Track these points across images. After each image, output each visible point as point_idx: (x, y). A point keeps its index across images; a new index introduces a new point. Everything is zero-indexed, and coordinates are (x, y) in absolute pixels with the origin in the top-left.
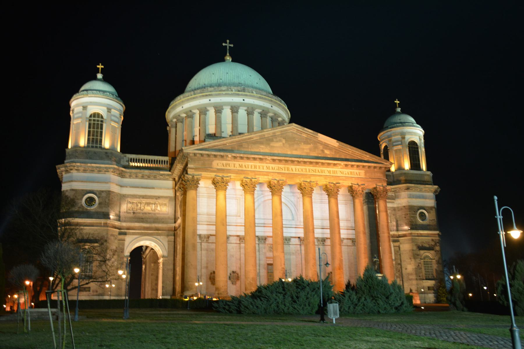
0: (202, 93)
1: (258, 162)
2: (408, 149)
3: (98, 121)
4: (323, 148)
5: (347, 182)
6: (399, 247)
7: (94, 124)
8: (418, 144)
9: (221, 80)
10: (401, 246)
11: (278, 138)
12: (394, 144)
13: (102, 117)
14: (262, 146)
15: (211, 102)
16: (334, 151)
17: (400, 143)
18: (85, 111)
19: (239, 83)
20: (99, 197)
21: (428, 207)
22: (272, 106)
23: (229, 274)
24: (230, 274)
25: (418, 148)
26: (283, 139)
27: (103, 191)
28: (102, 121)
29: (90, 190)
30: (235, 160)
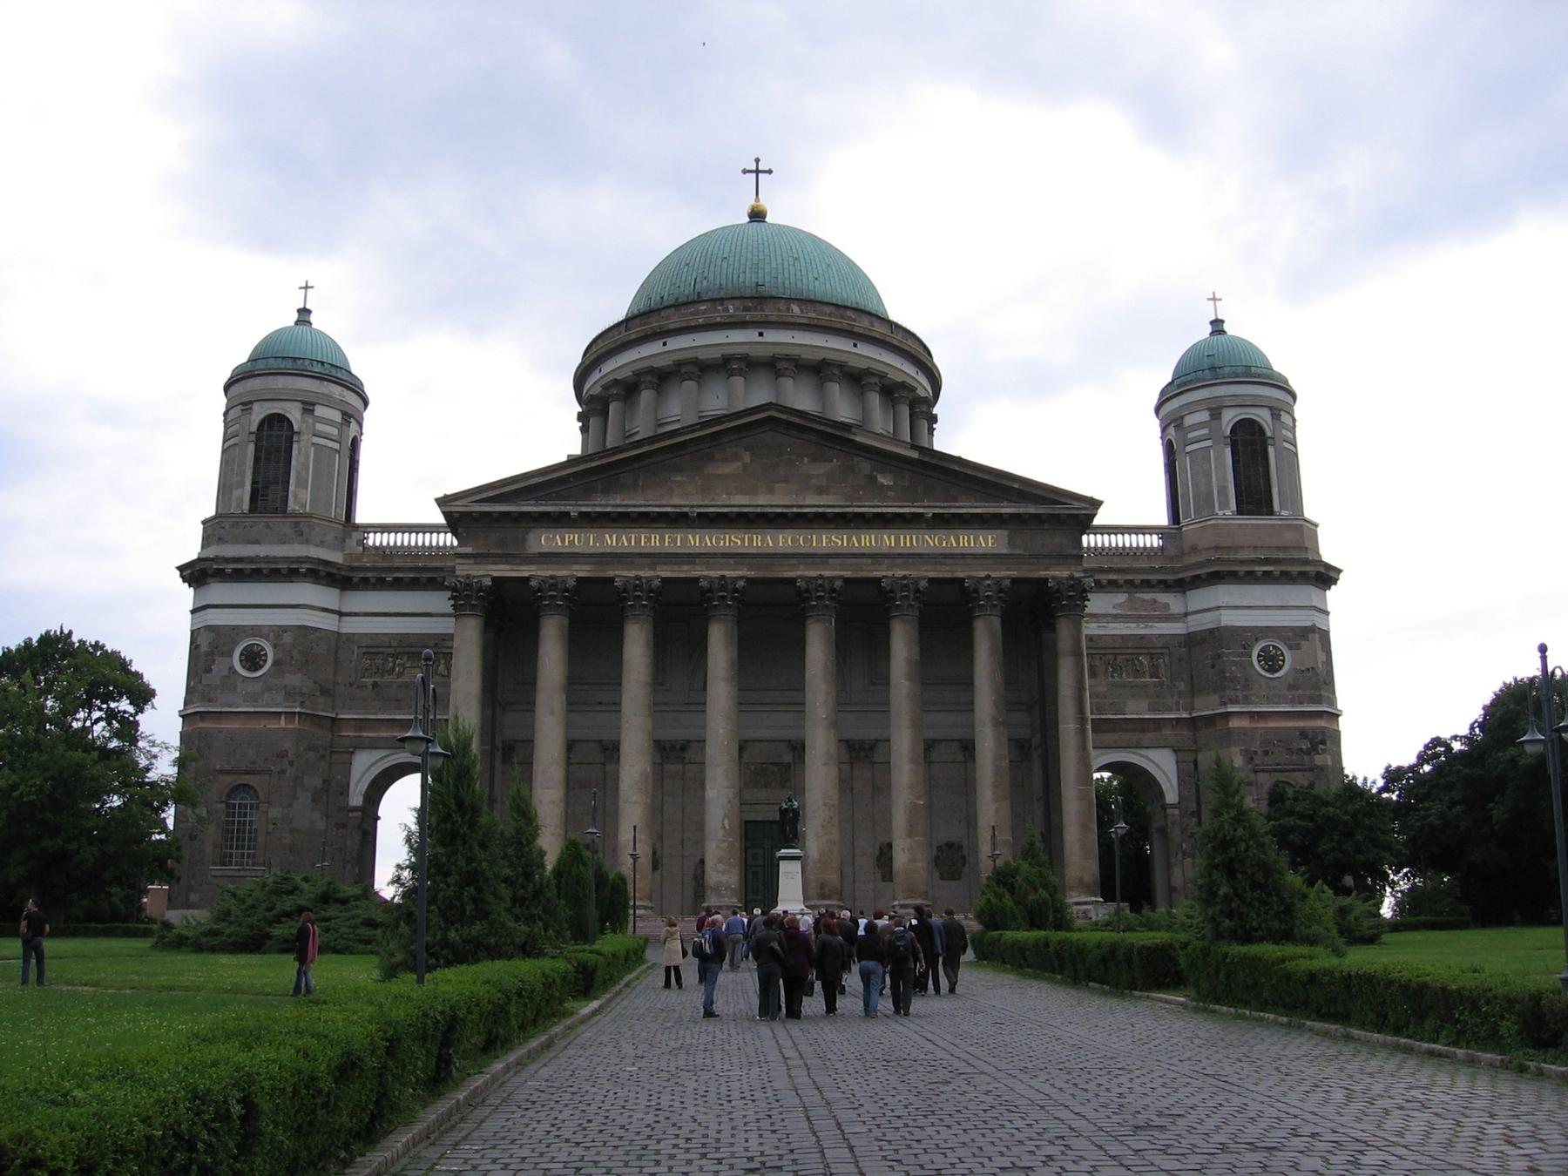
0: (645, 325)
2: (1228, 451)
4: (872, 472)
5: (947, 568)
6: (1195, 763)
8: (1269, 434)
9: (705, 281)
10: (1200, 757)
11: (728, 449)
12: (1191, 435)
14: (679, 478)
15: (666, 349)
17: (1206, 431)
19: (757, 285)
20: (275, 647)
21: (1292, 629)
22: (855, 345)
26: (746, 450)
27: (284, 629)
29: (252, 627)
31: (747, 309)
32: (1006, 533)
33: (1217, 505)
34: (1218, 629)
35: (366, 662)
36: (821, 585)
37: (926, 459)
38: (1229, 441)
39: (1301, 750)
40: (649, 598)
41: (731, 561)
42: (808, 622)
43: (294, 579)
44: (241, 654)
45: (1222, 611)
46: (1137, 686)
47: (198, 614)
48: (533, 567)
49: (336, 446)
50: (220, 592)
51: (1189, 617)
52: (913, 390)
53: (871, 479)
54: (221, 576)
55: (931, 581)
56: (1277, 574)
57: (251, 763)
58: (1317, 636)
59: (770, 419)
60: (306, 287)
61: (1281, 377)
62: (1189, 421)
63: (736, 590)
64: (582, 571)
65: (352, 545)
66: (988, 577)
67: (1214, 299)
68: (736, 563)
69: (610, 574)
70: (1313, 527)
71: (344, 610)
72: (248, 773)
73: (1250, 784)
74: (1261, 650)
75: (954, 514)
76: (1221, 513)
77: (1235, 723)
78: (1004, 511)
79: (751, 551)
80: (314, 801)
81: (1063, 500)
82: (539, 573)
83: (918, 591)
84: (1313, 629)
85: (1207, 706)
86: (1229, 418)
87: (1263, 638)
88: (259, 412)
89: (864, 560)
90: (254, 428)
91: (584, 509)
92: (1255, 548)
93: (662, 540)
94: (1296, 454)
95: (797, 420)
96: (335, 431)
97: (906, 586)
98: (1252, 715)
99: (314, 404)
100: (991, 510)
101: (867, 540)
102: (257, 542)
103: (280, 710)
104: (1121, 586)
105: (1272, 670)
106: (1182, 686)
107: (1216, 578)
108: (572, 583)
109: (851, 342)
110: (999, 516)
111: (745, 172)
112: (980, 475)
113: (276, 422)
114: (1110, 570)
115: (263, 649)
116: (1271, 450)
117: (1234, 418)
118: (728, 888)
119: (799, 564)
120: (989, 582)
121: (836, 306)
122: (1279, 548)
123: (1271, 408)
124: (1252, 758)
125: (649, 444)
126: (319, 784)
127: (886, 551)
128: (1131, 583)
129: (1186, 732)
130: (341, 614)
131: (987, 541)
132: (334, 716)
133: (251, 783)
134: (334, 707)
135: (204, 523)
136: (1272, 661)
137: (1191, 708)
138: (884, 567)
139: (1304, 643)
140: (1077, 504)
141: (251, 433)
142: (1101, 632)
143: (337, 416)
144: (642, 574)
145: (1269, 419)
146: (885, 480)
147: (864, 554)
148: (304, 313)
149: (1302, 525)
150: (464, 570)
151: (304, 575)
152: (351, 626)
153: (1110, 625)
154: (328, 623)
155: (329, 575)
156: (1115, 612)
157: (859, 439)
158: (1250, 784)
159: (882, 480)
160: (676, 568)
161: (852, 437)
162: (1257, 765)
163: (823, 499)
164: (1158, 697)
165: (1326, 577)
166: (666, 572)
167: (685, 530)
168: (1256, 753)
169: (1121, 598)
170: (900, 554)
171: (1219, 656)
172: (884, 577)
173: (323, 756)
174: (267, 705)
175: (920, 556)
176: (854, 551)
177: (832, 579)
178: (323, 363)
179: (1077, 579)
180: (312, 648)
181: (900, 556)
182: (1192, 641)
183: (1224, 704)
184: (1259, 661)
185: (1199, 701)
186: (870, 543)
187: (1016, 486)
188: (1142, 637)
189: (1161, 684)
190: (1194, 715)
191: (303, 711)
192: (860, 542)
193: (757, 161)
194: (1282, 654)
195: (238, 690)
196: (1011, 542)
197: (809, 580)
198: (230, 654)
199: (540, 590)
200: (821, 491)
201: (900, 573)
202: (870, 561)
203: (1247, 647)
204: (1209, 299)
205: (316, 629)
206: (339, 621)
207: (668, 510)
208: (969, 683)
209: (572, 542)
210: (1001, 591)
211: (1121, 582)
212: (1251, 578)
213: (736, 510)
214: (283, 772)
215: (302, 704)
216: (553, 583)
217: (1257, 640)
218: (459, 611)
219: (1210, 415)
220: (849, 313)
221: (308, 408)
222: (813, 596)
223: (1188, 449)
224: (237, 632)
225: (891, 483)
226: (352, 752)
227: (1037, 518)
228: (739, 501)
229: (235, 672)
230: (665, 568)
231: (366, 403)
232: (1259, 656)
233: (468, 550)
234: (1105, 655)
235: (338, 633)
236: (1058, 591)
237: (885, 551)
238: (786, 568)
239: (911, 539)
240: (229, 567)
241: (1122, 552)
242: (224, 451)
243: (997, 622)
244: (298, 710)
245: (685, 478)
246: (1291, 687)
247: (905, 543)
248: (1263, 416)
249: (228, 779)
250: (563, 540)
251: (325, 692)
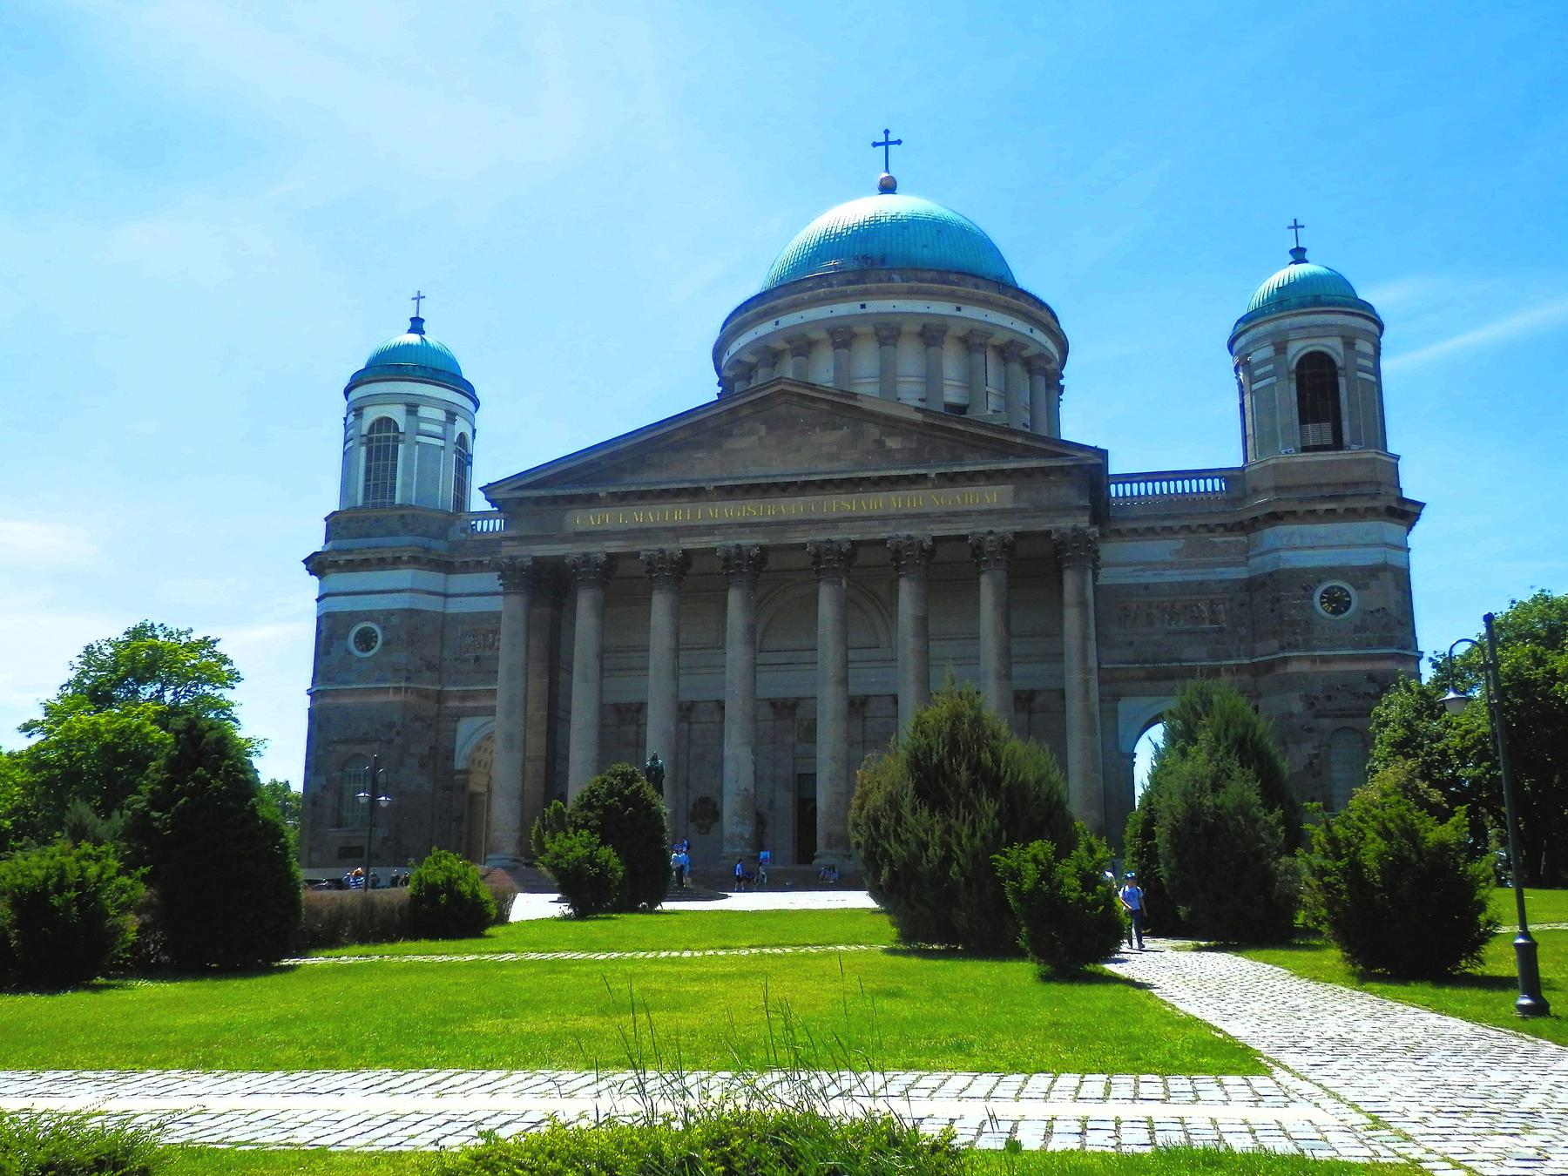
1: (685, 500)
2: (1293, 386)
3: (387, 438)
5: (953, 526)
7: (378, 447)
8: (1339, 363)
12: (1258, 372)
13: (396, 428)
14: (700, 455)
16: (915, 438)
17: (1270, 367)
18: (358, 421)
20: (384, 629)
21: (1361, 569)
22: (959, 309)
23: (691, 808)
24: (694, 806)
25: (1335, 376)
27: (390, 613)
28: (396, 440)
29: (364, 612)
30: (623, 503)
31: (849, 283)
32: (1010, 487)
33: (1280, 444)
34: (1277, 572)
35: (469, 640)
37: (930, 421)
38: (1294, 376)
39: (1369, 694)
40: (672, 569)
41: (747, 530)
42: (821, 584)
43: (401, 566)
44: (356, 637)
45: (1284, 554)
46: (1195, 633)
47: (323, 601)
48: (570, 546)
49: (440, 443)
50: (340, 581)
51: (1250, 561)
52: (1024, 347)
53: (880, 443)
54: (337, 567)
55: (934, 539)
56: (1341, 511)
57: (364, 734)
58: (1389, 575)
59: (783, 392)
60: (418, 298)
61: (1367, 306)
62: (1254, 358)
63: (750, 558)
64: (613, 547)
65: (456, 535)
66: (991, 533)
67: (1296, 226)
68: (751, 532)
69: (637, 548)
70: (1394, 461)
71: (451, 591)
72: (361, 741)
73: (1310, 730)
74: (1325, 592)
75: (956, 473)
76: (1283, 451)
77: (1293, 668)
78: (1005, 466)
79: (766, 519)
80: (421, 766)
81: (1066, 452)
82: (575, 550)
83: (922, 550)
84: (1385, 567)
85: (1267, 650)
86: (1297, 349)
87: (1326, 579)
88: (372, 414)
89: (873, 522)
90: (365, 431)
91: (611, 490)
92: (1320, 485)
93: (684, 514)
94: (1379, 384)
95: (807, 392)
96: (438, 430)
97: (909, 545)
98: (1313, 660)
99: (417, 406)
100: (994, 467)
101: (876, 502)
102: (368, 535)
103: (388, 685)
104: (1177, 533)
105: (1336, 612)
106: (1243, 631)
107: (1275, 518)
108: (603, 557)
109: (955, 305)
110: (1003, 471)
111: (875, 144)
112: (983, 432)
113: (385, 423)
114: (1165, 518)
115: (374, 631)
116: (1342, 381)
117: (1299, 351)
118: (743, 838)
120: (992, 538)
121: (938, 271)
122: (1346, 485)
123: (1343, 337)
124: (1313, 704)
125: (669, 425)
126: (426, 751)
128: (1188, 528)
129: (1246, 677)
130: (446, 595)
131: (993, 496)
132: (439, 688)
133: (364, 752)
134: (440, 682)
135: (326, 519)
136: (1338, 602)
137: (1252, 655)
138: (891, 528)
139: (1373, 583)
140: (1080, 455)
141: (362, 436)
142: (1157, 580)
143: (440, 415)
144: (665, 546)
145: (1340, 349)
146: (893, 443)
148: (417, 325)
149: (1375, 459)
150: (508, 550)
151: (408, 562)
152: (455, 607)
153: (1168, 572)
154: (432, 605)
155: (430, 561)
156: (1172, 559)
157: (866, 405)
158: (1310, 730)
159: (890, 444)
160: (697, 539)
161: (858, 404)
162: (1318, 711)
163: (836, 465)
164: (1217, 643)
165: (1408, 513)
166: (689, 544)
167: (705, 503)
168: (1316, 698)
169: (1178, 543)
171: (1278, 600)
172: (890, 538)
173: (430, 725)
174: (378, 681)
175: (926, 515)
176: (863, 513)
177: (840, 544)
178: (425, 368)
179: (1080, 529)
180: (417, 628)
181: (907, 516)
182: (1251, 586)
183: (1283, 648)
184: (1322, 603)
185: (1260, 647)
186: (878, 506)
187: (1019, 440)
188: (1201, 583)
189: (1221, 630)
190: (1254, 660)
191: (413, 685)
192: (868, 507)
193: (887, 132)
194: (1348, 595)
195: (353, 669)
196: (1016, 497)
197: (818, 544)
198: (346, 637)
199: (574, 566)
200: (832, 457)
201: (903, 533)
203: (1309, 590)
204: (1290, 228)
205: (419, 612)
206: (445, 602)
207: (687, 485)
208: (975, 637)
209: (603, 520)
210: (1004, 546)
211: (1176, 528)
212: (1312, 516)
213: (750, 482)
214: (391, 742)
215: (407, 679)
216: (587, 558)
217: (1320, 581)
218: (509, 588)
219: (1275, 350)
220: (952, 277)
221: (412, 409)
223: (1255, 387)
224: (354, 616)
225: (899, 446)
226: (458, 720)
227: (1041, 470)
228: (753, 472)
229: (350, 653)
230: (687, 540)
231: (477, 405)
232: (1322, 597)
233: (512, 533)
234: (1162, 602)
235: (444, 615)
236: (1062, 543)
237: (893, 511)
238: (799, 534)
239: (918, 499)
240: (342, 559)
241: (1170, 500)
242: (344, 453)
243: (1001, 574)
244: (403, 685)
245: (705, 455)
246: (1357, 629)
247: (912, 504)
248: (1332, 346)
249: (341, 749)
250: (596, 521)
251: (431, 667)
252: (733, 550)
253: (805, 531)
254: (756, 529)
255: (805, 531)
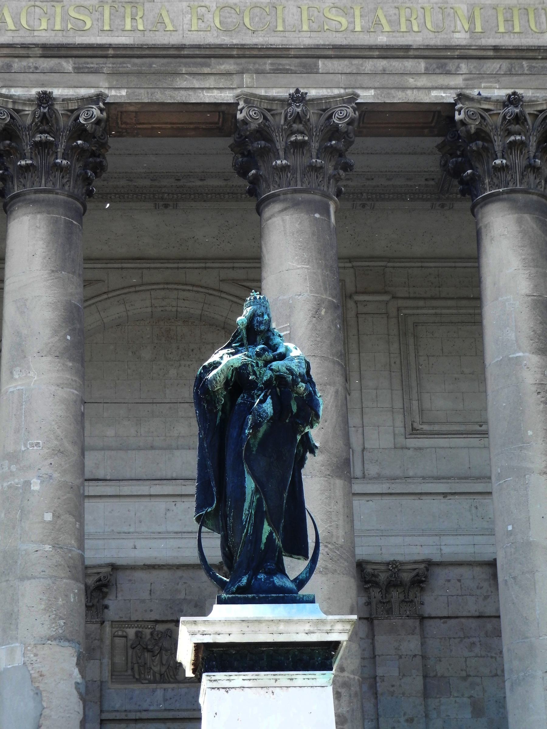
36: (298, 118)
41: (68, 65)
42: (268, 212)
68: (78, 70)
89: (409, 64)
119: (241, 72)
127: (464, 43)
138: (458, 81)
147: (407, 48)
170: (496, 48)
176: (382, 40)
202: (422, 65)
222: (280, 145)
238: (210, 82)
252: (29, 110)
253: (228, 74)
254: (94, 63)
255: (228, 74)
